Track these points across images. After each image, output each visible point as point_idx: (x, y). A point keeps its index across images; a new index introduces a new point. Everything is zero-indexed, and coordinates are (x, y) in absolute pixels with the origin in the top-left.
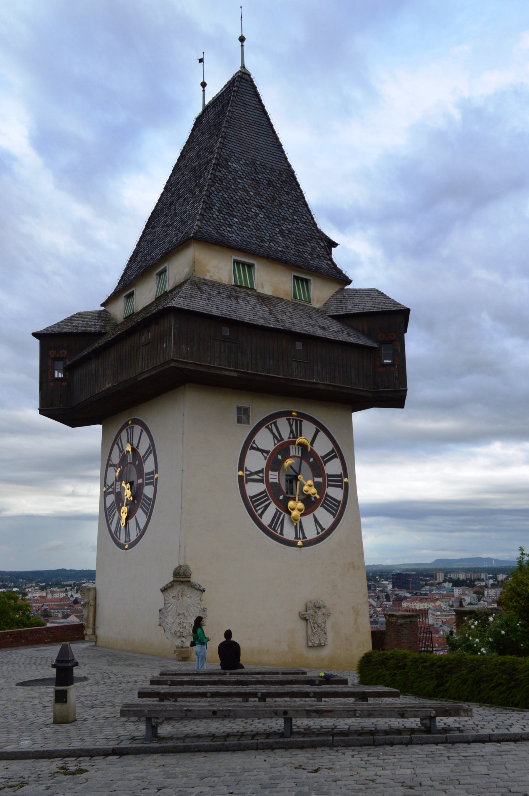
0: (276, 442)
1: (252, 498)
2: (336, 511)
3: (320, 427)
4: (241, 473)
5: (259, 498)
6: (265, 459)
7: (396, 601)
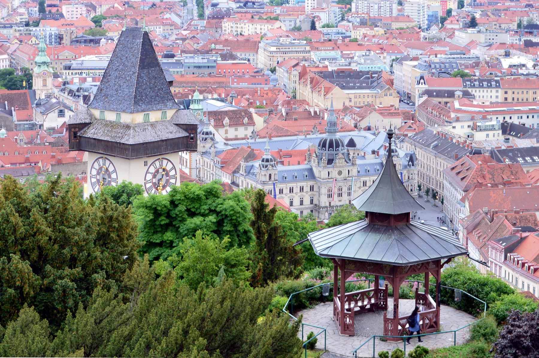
5: (150, 188)
7: (213, 18)
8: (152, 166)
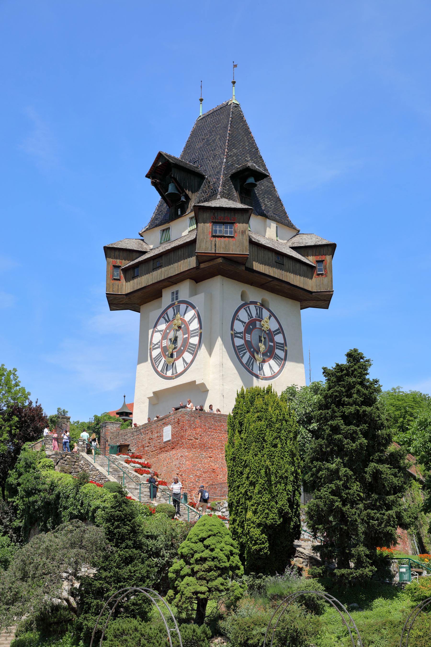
1: (237, 347)
3: (272, 314)
4: (232, 332)
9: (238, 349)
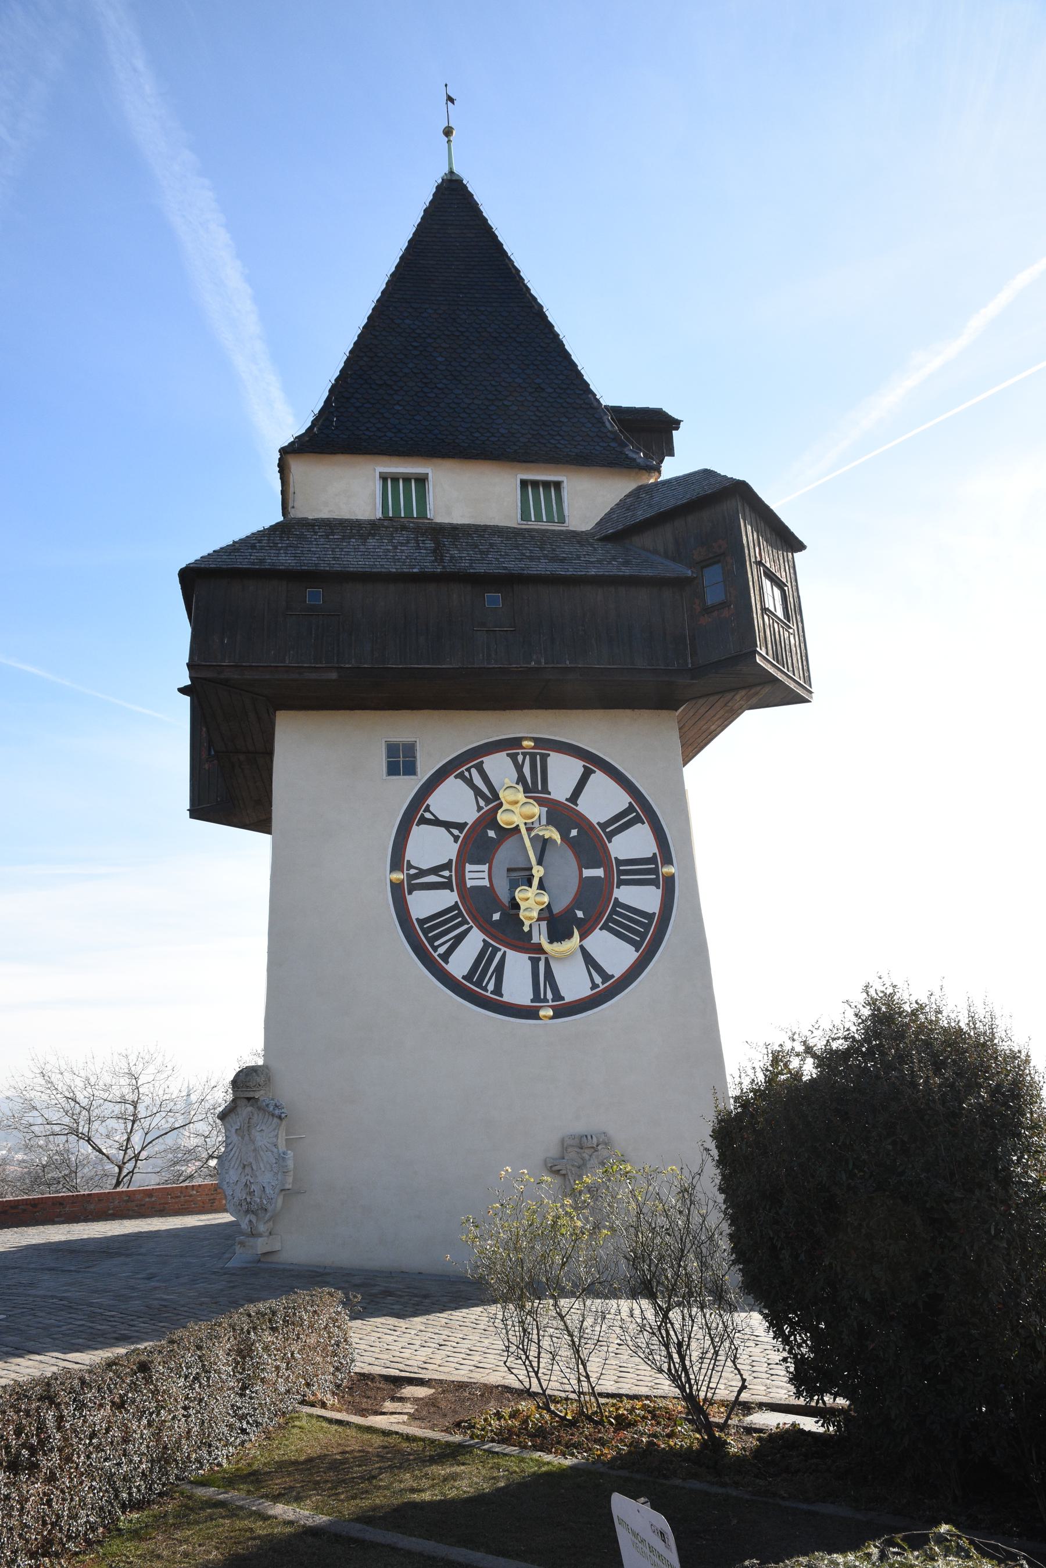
0: (482, 803)
2: (643, 936)
6: (456, 841)
8: (452, 785)
9: (425, 932)
